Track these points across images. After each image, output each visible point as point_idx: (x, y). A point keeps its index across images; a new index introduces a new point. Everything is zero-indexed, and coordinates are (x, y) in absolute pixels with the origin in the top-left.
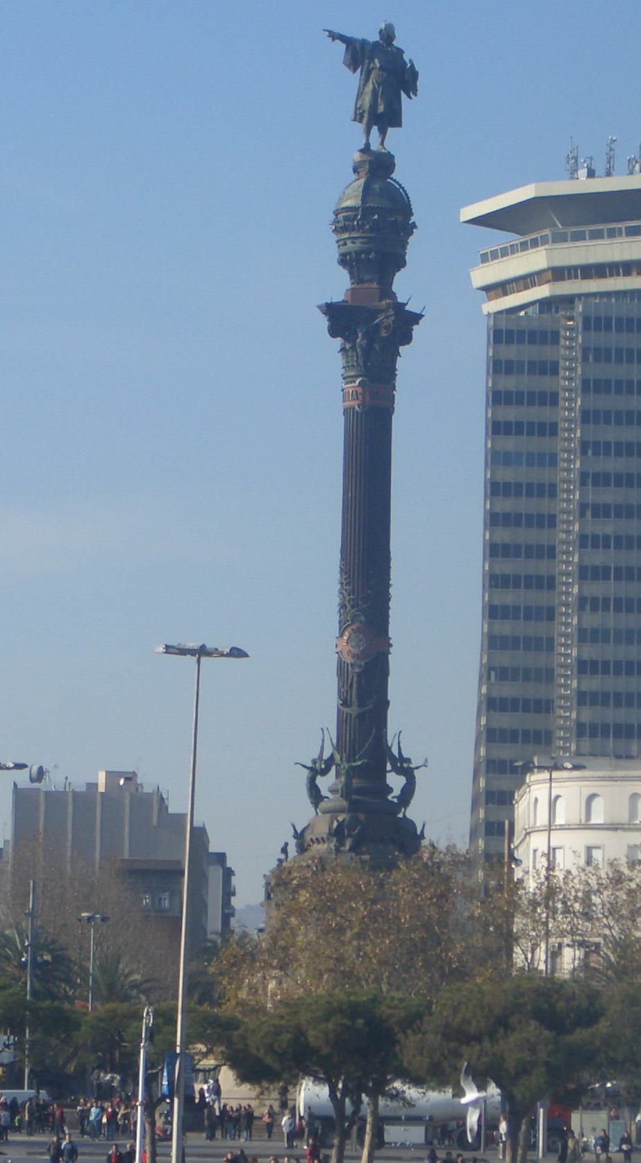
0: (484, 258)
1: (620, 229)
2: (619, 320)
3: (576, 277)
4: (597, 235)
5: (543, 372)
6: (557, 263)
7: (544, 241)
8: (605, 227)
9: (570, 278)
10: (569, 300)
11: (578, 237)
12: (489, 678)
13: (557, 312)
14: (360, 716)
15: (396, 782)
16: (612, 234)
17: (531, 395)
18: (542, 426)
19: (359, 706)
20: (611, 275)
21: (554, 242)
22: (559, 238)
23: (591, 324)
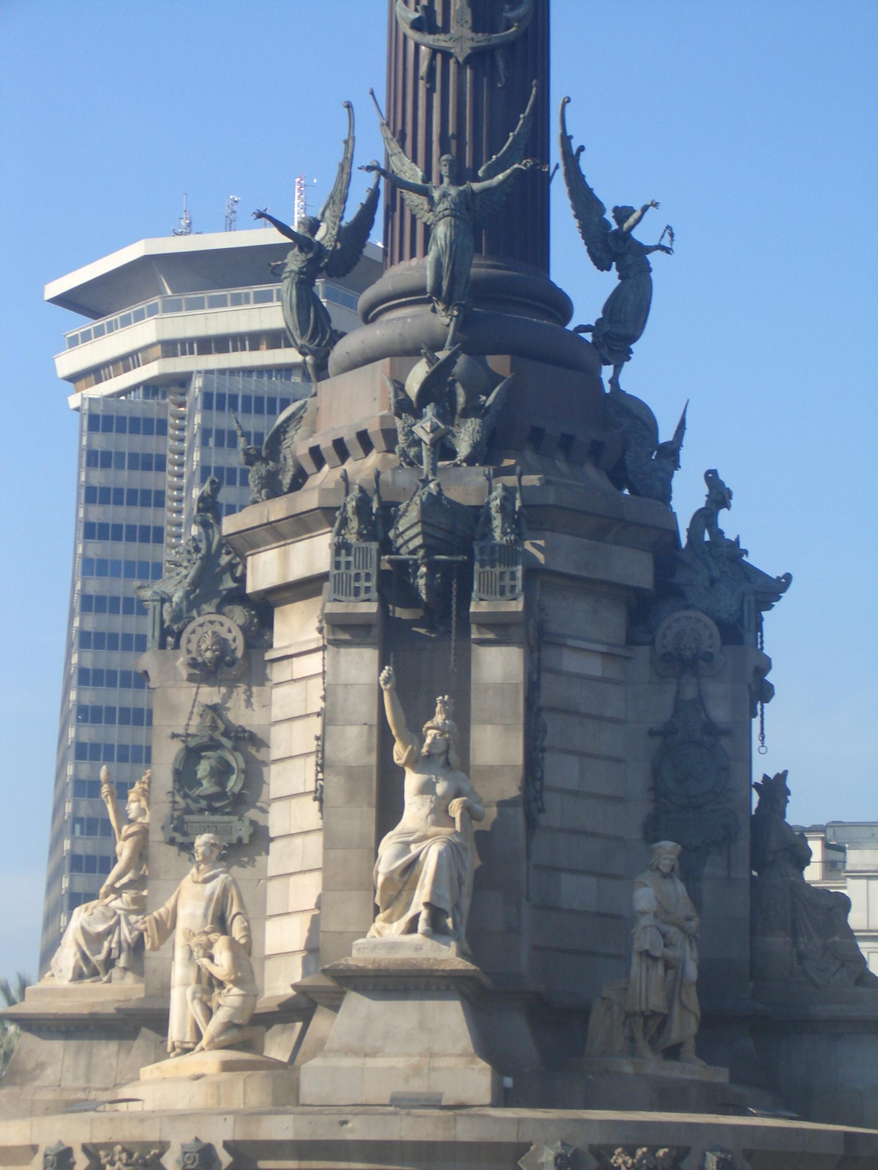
0: (73, 342)
1: (247, 295)
2: (247, 399)
3: (192, 353)
4: (219, 303)
5: (147, 467)
6: (169, 335)
7: (153, 311)
8: (228, 292)
9: (184, 353)
10: (182, 381)
11: (196, 305)
12: (73, 832)
13: (164, 397)
14: (479, 59)
15: (584, 286)
16: (237, 301)
17: (132, 493)
18: (145, 530)
19: (475, 29)
20: (235, 350)
21: (164, 311)
22: (172, 307)
23: (213, 401)
